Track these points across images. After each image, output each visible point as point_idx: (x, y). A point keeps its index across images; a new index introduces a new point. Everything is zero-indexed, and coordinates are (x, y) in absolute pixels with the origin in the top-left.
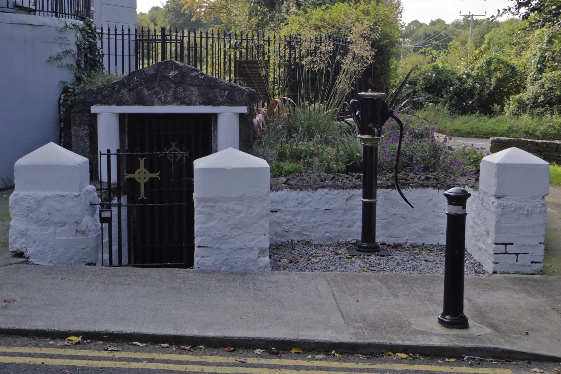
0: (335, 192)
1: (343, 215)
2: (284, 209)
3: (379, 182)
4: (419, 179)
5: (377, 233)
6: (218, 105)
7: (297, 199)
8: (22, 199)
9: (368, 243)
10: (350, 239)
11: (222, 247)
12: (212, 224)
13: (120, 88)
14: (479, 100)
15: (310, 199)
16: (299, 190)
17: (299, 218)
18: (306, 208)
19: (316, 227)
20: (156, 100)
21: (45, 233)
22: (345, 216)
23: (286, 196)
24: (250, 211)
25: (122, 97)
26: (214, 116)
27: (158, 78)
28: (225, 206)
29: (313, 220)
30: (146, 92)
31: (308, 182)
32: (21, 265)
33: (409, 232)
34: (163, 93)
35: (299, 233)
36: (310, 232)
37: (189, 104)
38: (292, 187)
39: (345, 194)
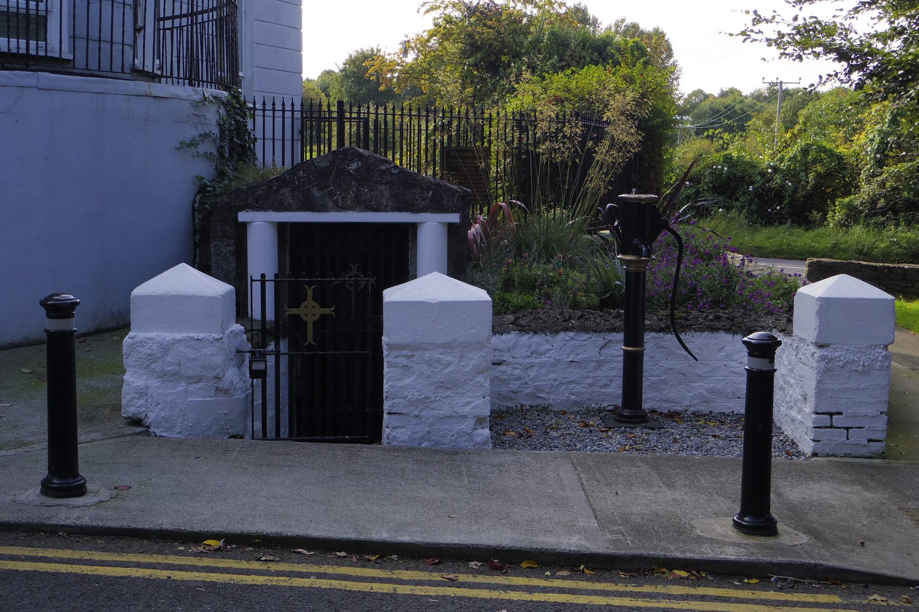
0: (585, 336)
1: (596, 370)
3: (647, 322)
4: (705, 319)
7: (530, 346)
8: (141, 343)
9: (631, 410)
10: (605, 404)
11: (423, 413)
12: (408, 381)
14: (791, 205)
15: (548, 346)
17: (533, 373)
18: (543, 359)
20: (330, 204)
22: (599, 372)
24: (463, 363)
28: (428, 355)
29: (553, 376)
30: (316, 193)
31: (545, 322)
32: (138, 437)
35: (532, 395)
36: (548, 393)
37: (377, 210)
38: (522, 329)
39: (598, 339)
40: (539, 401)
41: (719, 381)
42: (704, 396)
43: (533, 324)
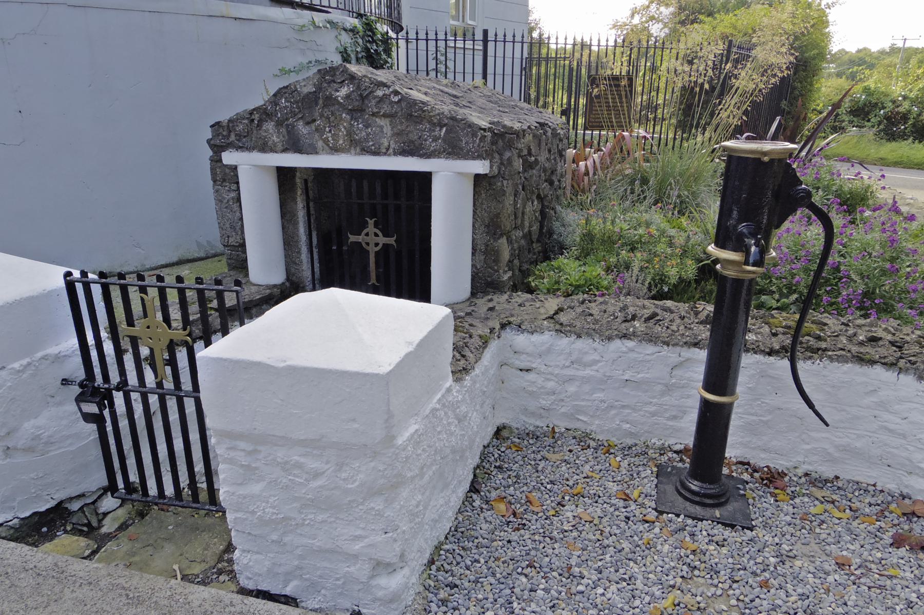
0: (650, 349)
1: (663, 394)
2: (543, 368)
3: (750, 337)
4: (850, 338)
7: (570, 354)
9: (705, 474)
10: (671, 441)
11: (287, 539)
12: (256, 488)
13: (261, 121)
14: (914, 125)
16: (574, 337)
17: (572, 389)
18: (588, 372)
19: (604, 410)
20: (320, 144)
22: (667, 398)
23: (547, 345)
24: (344, 475)
25: (266, 137)
26: (425, 179)
27: (321, 102)
28: (280, 454)
29: (600, 395)
30: (302, 129)
31: (596, 322)
33: (808, 447)
34: (330, 131)
35: (571, 416)
36: (592, 416)
37: (376, 153)
38: (562, 330)
39: (671, 355)
40: (578, 425)
41: (859, 436)
43: (579, 325)
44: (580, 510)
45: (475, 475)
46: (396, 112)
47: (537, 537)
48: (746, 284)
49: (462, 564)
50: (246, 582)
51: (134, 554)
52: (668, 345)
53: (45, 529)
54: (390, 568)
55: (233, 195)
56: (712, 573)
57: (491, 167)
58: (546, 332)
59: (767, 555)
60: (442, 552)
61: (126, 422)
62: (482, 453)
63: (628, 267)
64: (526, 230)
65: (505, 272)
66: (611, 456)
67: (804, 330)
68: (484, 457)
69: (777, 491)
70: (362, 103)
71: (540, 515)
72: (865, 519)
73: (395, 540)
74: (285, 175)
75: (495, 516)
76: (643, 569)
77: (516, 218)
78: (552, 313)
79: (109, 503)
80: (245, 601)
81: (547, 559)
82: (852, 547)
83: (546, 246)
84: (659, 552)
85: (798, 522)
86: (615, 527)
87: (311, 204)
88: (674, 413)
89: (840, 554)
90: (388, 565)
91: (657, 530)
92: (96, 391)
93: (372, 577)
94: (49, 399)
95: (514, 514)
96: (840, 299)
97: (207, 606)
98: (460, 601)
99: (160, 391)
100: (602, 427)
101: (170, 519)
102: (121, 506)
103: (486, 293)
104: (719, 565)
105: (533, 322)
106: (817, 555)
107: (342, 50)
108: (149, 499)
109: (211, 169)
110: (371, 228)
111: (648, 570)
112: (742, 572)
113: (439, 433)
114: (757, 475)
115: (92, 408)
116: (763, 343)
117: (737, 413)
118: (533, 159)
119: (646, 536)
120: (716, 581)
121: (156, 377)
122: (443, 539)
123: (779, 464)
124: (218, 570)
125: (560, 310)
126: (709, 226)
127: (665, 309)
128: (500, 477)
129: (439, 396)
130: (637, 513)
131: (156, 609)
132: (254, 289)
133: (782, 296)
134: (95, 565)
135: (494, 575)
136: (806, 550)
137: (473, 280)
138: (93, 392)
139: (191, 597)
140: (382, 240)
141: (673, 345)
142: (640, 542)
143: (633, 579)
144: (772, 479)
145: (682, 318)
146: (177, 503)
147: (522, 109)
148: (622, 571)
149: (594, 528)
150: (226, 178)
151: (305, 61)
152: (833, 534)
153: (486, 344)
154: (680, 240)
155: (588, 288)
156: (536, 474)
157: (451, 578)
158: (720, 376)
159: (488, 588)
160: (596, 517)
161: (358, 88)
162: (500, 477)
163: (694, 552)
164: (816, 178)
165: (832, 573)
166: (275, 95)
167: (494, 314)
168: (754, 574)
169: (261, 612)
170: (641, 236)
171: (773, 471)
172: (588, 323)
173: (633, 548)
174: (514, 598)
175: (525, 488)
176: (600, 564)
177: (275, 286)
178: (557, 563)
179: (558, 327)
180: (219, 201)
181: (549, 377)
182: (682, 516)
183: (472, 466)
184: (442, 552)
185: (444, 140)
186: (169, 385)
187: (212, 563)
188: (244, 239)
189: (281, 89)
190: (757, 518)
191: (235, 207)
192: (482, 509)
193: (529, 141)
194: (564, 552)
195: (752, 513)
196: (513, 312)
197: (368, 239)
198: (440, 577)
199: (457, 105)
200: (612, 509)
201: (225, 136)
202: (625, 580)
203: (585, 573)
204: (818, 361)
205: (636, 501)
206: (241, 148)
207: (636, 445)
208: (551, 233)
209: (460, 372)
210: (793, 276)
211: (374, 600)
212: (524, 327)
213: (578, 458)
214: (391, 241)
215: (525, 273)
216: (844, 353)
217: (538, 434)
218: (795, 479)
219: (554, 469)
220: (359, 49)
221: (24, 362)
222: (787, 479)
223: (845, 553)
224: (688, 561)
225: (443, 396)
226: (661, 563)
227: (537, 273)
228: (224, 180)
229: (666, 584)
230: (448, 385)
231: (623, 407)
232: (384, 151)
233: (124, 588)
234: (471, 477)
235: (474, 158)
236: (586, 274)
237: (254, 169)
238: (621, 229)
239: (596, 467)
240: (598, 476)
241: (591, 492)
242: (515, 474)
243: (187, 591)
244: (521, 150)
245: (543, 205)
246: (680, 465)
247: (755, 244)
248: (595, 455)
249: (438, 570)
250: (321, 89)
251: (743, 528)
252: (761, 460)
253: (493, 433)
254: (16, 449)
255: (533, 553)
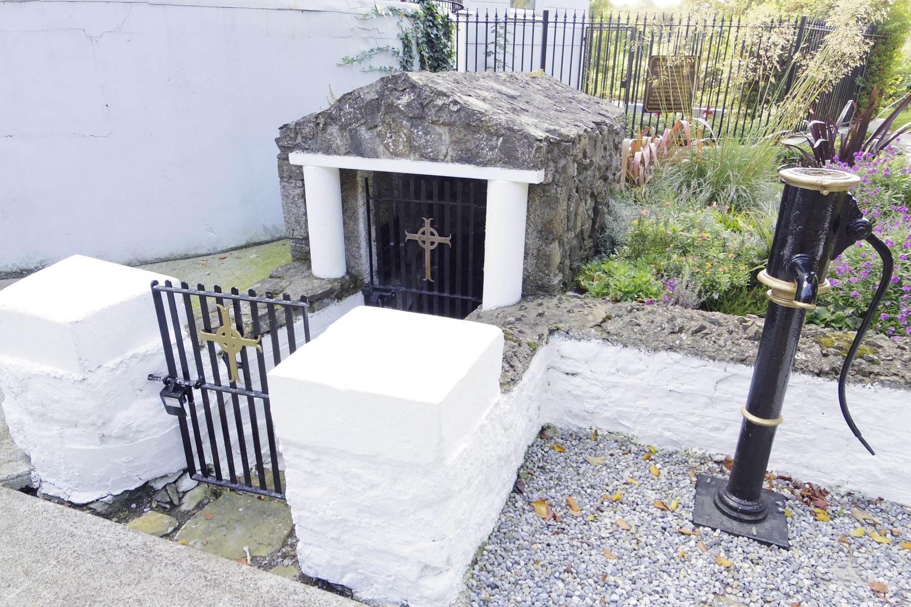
0: (696, 362)
1: (706, 406)
2: (588, 374)
3: (800, 356)
5: (773, 454)
6: (485, 164)
7: (616, 362)
9: (745, 488)
10: (712, 452)
15: (641, 366)
16: (620, 346)
17: (616, 394)
18: (632, 380)
20: (381, 148)
21: (48, 434)
25: (330, 140)
26: (481, 185)
27: (383, 109)
29: (643, 403)
30: (364, 134)
31: (643, 332)
34: (391, 137)
35: (614, 421)
37: (434, 160)
39: (716, 369)
40: (620, 429)
42: (874, 476)
43: (625, 334)
44: (618, 517)
45: (518, 475)
46: (454, 122)
47: (575, 543)
48: (797, 313)
49: (503, 565)
50: (308, 570)
51: (210, 533)
52: (714, 360)
53: (134, 506)
54: (437, 571)
55: (298, 191)
56: (745, 592)
57: (546, 175)
58: (593, 340)
59: (801, 576)
60: (485, 553)
61: (203, 411)
62: (527, 453)
63: (678, 272)
64: (578, 230)
65: (555, 275)
66: (652, 463)
67: (858, 352)
68: (528, 457)
69: (817, 510)
70: (423, 110)
71: (579, 519)
72: (905, 545)
73: (442, 548)
74: (347, 177)
75: (536, 518)
76: (676, 582)
77: (568, 221)
78: (600, 320)
79: (187, 483)
80: (307, 590)
81: (583, 566)
82: (889, 574)
83: (598, 243)
84: (693, 566)
85: (836, 544)
86: (651, 537)
87: (371, 201)
88: (716, 425)
89: (877, 580)
90: (434, 569)
91: (692, 543)
92: (178, 388)
93: (420, 577)
94: (138, 392)
95: (555, 517)
96: (899, 316)
97: (274, 593)
98: (500, 602)
99: (234, 390)
100: (646, 433)
101: (242, 502)
102: (198, 485)
103: (536, 296)
104: (752, 584)
105: (581, 329)
106: (853, 579)
107: (403, 36)
108: (223, 483)
109: (279, 166)
110: (427, 227)
111: (682, 584)
112: (774, 593)
113: (487, 445)
114: (797, 491)
115: (175, 403)
116: (813, 364)
117: (781, 430)
118: (588, 161)
119: (683, 549)
120: (747, 600)
121: (230, 378)
122: (486, 539)
123: (822, 482)
124: (283, 554)
125: (609, 318)
126: (766, 231)
127: (713, 322)
128: (543, 478)
129: (487, 412)
130: (674, 524)
131: (230, 593)
132: (316, 283)
133: (837, 307)
134: (178, 547)
135: (532, 577)
136: (842, 573)
137: (524, 282)
138: (175, 388)
139: (260, 583)
140: (438, 239)
141: (720, 360)
142: (675, 555)
143: (666, 592)
144: (813, 496)
145: (731, 332)
146: (247, 488)
147: (579, 102)
148: (655, 583)
149: (631, 537)
150: (293, 177)
151: (367, 49)
152: (871, 559)
153: (534, 349)
154: (734, 242)
155: (636, 295)
156: (577, 477)
157: (492, 579)
158: (765, 397)
159: (527, 590)
160: (633, 526)
161: (419, 96)
162: (543, 478)
163: (728, 569)
164: (886, 175)
165: (866, 599)
166: (340, 101)
167: (544, 319)
168: (787, 595)
169: (321, 602)
170: (694, 239)
171: (815, 488)
172: (635, 333)
173: (667, 560)
174: (551, 603)
175: (566, 491)
176: (634, 574)
177: (336, 280)
178: (593, 570)
179: (605, 335)
180: (285, 196)
181: (593, 382)
182: (718, 531)
183: (516, 469)
184: (485, 553)
185: (500, 150)
186: (241, 384)
187: (278, 547)
188: (308, 233)
189: (345, 95)
190: (794, 538)
191: (300, 202)
192: (524, 510)
193: (585, 145)
194: (600, 559)
195: (790, 532)
196: (562, 318)
197: (424, 238)
198: (482, 578)
199: (514, 110)
200: (649, 519)
201: (293, 137)
202: (658, 593)
203: (620, 582)
204: (869, 385)
205: (673, 512)
206: (307, 149)
207: (677, 452)
208: (603, 229)
209: (508, 383)
210: (851, 288)
211: (422, 598)
212: (571, 334)
213: (618, 462)
214: (446, 240)
215: (575, 271)
216: (895, 378)
217: (581, 435)
218: (837, 498)
219: (594, 473)
220: (419, 35)
221: (118, 360)
222: (828, 497)
223: (881, 579)
224: (722, 577)
225: (491, 411)
226: (694, 578)
227: (587, 272)
228: (290, 177)
229: (698, 600)
230: (496, 400)
231: (666, 415)
232: (442, 157)
233: (202, 570)
234: (515, 477)
235: (529, 169)
236: (636, 280)
237: (319, 170)
238: (674, 231)
239: (636, 474)
240: (637, 483)
241: (630, 499)
242: (556, 476)
243: (256, 577)
244: (576, 156)
245: (596, 202)
246: (720, 476)
247: (807, 279)
248: (636, 461)
249: (481, 570)
250: (383, 96)
251: (779, 547)
252: (803, 476)
253: (537, 432)
254: (110, 436)
255: (571, 558)
